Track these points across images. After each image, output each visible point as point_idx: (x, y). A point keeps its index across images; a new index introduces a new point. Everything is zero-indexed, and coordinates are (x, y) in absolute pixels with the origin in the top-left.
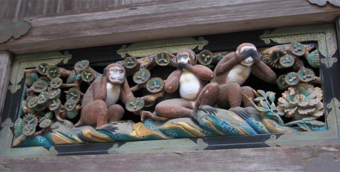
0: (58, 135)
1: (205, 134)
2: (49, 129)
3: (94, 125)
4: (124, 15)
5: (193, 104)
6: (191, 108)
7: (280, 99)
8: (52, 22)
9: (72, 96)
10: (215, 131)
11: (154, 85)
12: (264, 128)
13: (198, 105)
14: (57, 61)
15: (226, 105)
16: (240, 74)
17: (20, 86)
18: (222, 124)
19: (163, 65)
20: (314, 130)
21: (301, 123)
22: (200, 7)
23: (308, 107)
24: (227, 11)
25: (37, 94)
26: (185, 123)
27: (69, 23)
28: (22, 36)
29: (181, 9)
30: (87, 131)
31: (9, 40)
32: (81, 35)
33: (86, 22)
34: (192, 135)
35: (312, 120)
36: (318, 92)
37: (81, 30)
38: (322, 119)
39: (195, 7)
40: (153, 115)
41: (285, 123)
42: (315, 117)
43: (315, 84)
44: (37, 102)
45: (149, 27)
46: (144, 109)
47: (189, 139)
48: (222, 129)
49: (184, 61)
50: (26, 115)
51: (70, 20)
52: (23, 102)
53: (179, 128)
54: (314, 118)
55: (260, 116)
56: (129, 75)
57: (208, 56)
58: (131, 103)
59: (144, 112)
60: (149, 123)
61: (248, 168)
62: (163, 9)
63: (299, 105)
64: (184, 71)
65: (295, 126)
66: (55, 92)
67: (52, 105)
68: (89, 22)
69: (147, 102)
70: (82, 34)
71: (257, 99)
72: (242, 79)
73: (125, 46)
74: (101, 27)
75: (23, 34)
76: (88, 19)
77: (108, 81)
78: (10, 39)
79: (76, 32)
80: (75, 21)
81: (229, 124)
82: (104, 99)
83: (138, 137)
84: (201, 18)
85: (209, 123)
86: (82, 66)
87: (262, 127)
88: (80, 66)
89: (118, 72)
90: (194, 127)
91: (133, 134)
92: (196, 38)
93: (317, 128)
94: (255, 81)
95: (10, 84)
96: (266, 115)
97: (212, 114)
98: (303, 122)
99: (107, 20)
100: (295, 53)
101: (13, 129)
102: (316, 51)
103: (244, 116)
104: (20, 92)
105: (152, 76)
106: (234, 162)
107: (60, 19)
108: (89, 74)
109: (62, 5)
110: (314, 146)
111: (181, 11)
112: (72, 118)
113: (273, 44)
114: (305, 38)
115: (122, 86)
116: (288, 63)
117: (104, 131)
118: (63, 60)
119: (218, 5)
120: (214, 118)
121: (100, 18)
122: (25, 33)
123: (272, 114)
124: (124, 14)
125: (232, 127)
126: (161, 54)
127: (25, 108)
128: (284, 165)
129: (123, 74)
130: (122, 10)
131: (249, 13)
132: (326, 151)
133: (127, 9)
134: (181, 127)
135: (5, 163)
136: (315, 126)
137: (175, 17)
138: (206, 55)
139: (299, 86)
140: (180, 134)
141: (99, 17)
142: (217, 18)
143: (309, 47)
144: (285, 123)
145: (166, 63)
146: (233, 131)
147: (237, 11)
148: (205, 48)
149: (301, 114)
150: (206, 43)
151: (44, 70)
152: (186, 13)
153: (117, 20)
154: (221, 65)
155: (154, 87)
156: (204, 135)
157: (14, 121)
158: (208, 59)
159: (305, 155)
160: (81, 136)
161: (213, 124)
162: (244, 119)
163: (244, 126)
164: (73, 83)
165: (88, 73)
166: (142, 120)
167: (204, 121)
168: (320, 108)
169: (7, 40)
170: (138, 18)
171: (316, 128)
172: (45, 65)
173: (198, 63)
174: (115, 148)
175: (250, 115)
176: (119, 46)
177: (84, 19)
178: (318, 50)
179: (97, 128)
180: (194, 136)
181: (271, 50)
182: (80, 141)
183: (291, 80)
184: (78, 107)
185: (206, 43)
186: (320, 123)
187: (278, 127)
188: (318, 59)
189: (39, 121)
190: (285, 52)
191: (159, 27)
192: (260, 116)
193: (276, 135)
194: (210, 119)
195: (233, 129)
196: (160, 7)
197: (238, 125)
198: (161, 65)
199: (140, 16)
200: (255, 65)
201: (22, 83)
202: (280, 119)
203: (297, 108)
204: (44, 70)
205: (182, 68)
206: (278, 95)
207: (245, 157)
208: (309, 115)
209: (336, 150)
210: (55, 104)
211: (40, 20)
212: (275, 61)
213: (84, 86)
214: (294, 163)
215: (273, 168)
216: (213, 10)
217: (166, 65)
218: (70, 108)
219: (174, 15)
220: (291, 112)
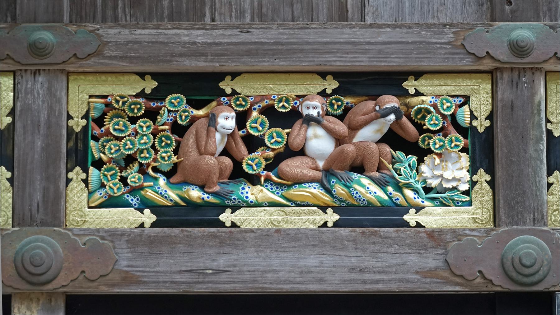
2: (141, 188)
4: (233, 40)
5: (321, 164)
7: (424, 168)
8: (131, 38)
9: (163, 141)
11: (273, 138)
15: (360, 169)
16: (378, 131)
17: (84, 122)
19: (284, 111)
22: (333, 40)
23: (454, 179)
24: (366, 49)
25: (119, 139)
27: (157, 42)
28: (89, 55)
29: (309, 40)
30: (195, 194)
31: (70, 58)
33: (181, 43)
36: (465, 160)
37: (174, 56)
38: (467, 193)
39: (328, 40)
41: (426, 193)
43: (464, 150)
44: (119, 150)
45: (268, 61)
46: (267, 168)
50: (105, 166)
51: (156, 37)
52: (92, 143)
57: (340, 103)
58: (250, 162)
59: (265, 172)
61: (389, 250)
62: (286, 37)
63: (444, 176)
64: (311, 125)
66: (145, 138)
67: (142, 155)
68: (185, 43)
69: (266, 159)
70: (177, 61)
71: (396, 166)
72: (379, 136)
73: (229, 78)
75: (91, 53)
77: (216, 130)
78: (71, 57)
79: (168, 58)
80: (166, 41)
82: (213, 155)
83: (257, 203)
84: (334, 57)
86: (176, 104)
88: (172, 103)
95: (69, 117)
99: (210, 44)
101: (86, 182)
102: (466, 107)
103: (382, 184)
104: (85, 129)
105: (270, 127)
106: (374, 243)
107: (140, 34)
111: (308, 43)
112: (166, 171)
113: (418, 94)
115: (231, 136)
117: (215, 194)
118: (145, 88)
119: (356, 40)
121: (200, 40)
122: (94, 51)
124: (232, 37)
126: (282, 98)
127: (102, 155)
128: (426, 248)
129: (234, 120)
130: (229, 32)
131: (394, 56)
133: (236, 31)
135: (100, 234)
137: (302, 51)
138: (337, 100)
141: (199, 38)
142: (355, 59)
144: (426, 193)
147: (380, 52)
148: (335, 92)
149: (445, 188)
151: (121, 103)
152: (315, 47)
153: (225, 47)
154: (356, 116)
157: (86, 171)
164: (162, 125)
165: (184, 113)
169: (68, 58)
170: (253, 46)
172: (122, 97)
173: (327, 113)
176: (221, 76)
177: (177, 39)
178: (469, 106)
179: (206, 190)
182: (183, 204)
183: (437, 146)
184: (174, 159)
189: (124, 174)
190: (432, 109)
196: (282, 34)
198: (280, 110)
199: (255, 43)
201: (86, 116)
203: (440, 179)
204: (121, 103)
205: (309, 120)
206: (421, 161)
207: (386, 238)
208: (455, 188)
209: (480, 235)
210: (145, 154)
211: (111, 31)
212: (419, 117)
214: (435, 247)
215: (415, 251)
216: (350, 47)
219: (300, 47)
220: (434, 183)
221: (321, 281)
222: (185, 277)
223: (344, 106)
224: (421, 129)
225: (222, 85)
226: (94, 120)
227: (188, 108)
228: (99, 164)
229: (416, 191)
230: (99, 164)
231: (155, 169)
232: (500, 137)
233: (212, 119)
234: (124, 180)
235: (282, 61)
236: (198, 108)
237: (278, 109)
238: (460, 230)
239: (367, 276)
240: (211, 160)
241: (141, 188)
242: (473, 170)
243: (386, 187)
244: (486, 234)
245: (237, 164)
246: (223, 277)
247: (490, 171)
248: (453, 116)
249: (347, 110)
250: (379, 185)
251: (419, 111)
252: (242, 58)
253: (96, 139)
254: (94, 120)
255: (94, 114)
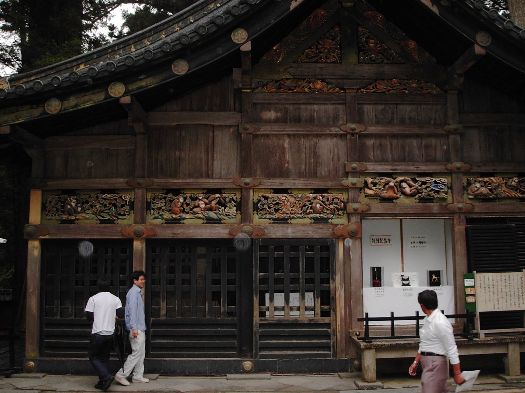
0: (165, 216)
2: (163, 215)
3: (176, 214)
5: (203, 209)
6: (202, 210)
13: (204, 210)
14: (162, 193)
26: (201, 215)
30: (174, 216)
36: (235, 208)
38: (235, 216)
40: (191, 212)
43: (235, 206)
49: (200, 198)
52: (152, 205)
55: (220, 215)
56: (185, 199)
69: (190, 208)
76: (172, 181)
91: (187, 217)
92: (204, 189)
94: (219, 203)
95: (147, 199)
96: (222, 214)
101: (150, 213)
103: (216, 213)
104: (150, 201)
113: (224, 193)
114: (233, 192)
139: (230, 208)
140: (199, 218)
143: (234, 195)
148: (206, 193)
154: (210, 199)
157: (150, 211)
159: (230, 226)
160: (172, 217)
167: (206, 216)
173: (204, 198)
174: (182, 221)
176: (181, 189)
181: (224, 195)
185: (206, 191)
192: (220, 215)
200: (220, 200)
201: (151, 199)
205: (200, 200)
206: (225, 209)
211: (156, 180)
213: (171, 201)
221: (201, 236)
222: (171, 235)
224: (225, 201)
225: (181, 191)
226: (153, 199)
227: (173, 197)
228: (153, 209)
229: (224, 215)
230: (153, 209)
231: (166, 211)
232: (242, 203)
233: (178, 199)
234: (159, 213)
236: (176, 196)
239: (212, 235)
240: (177, 209)
241: (163, 215)
242: (237, 211)
245: (184, 209)
246: (179, 235)
247: (241, 211)
248: (233, 198)
249: (209, 197)
251: (225, 197)
253: (153, 203)
254: (153, 199)
255: (152, 198)
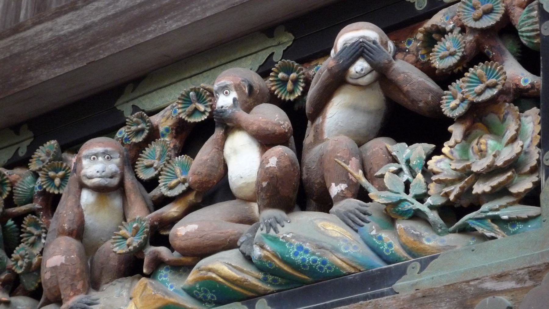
1: (271, 284)
10: (284, 270)
12: (396, 247)
18: (296, 254)
20: (514, 233)
21: (477, 219)
32: (30, 83)
34: (245, 292)
35: (506, 206)
42: (518, 194)
47: (239, 304)
48: (299, 265)
53: (211, 279)
54: (511, 200)
59: (151, 249)
60: (165, 276)
65: (465, 230)
70: (31, 79)
74: (67, 54)
81: (311, 249)
85: (266, 257)
87: (390, 245)
89: (100, 159)
90: (242, 271)
93: (521, 226)
97: (272, 232)
98: (483, 215)
99: (79, 31)
100: (471, 24)
108: (61, 173)
109: (29, 7)
110: (468, 282)
116: (452, 54)
120: (275, 240)
123: (411, 206)
125: (319, 256)
126: (188, 93)
132: (493, 293)
134: (214, 275)
136: (512, 221)
145: (203, 113)
146: (325, 268)
150: (287, 39)
155: (174, 182)
156: (269, 288)
158: (295, 82)
161: (276, 256)
162: (356, 231)
163: (351, 250)
166: (145, 271)
168: (528, 169)
170: (136, 12)
171: (520, 226)
175: (367, 218)
180: (250, 294)
185: (287, 39)
186: (531, 210)
187: (428, 240)
188: (537, 26)
191: (174, 26)
193: (420, 261)
194: (269, 246)
195: (324, 262)
197: (335, 250)
198: (192, 120)
202: (433, 216)
209: (519, 286)
217: (204, 117)
218: (21, 267)
223: (302, 81)
235: (177, 21)
237: (186, 119)
238: (472, 283)
243: (362, 226)
244: (531, 279)
250: (353, 224)
252: (119, 39)
